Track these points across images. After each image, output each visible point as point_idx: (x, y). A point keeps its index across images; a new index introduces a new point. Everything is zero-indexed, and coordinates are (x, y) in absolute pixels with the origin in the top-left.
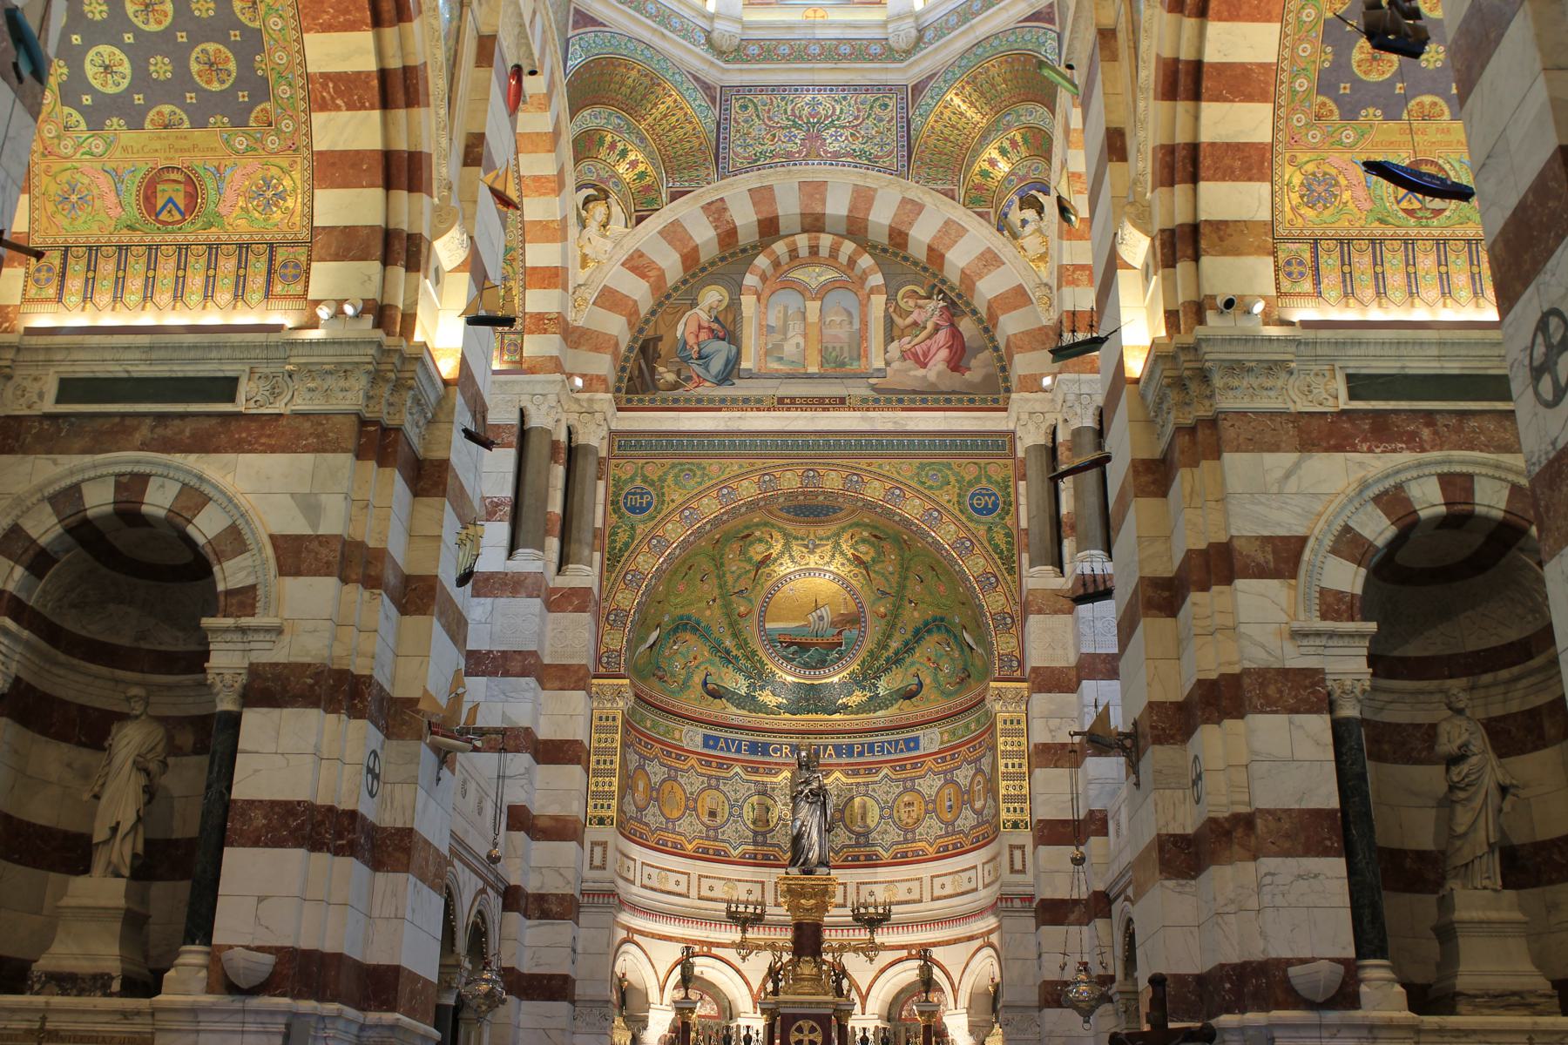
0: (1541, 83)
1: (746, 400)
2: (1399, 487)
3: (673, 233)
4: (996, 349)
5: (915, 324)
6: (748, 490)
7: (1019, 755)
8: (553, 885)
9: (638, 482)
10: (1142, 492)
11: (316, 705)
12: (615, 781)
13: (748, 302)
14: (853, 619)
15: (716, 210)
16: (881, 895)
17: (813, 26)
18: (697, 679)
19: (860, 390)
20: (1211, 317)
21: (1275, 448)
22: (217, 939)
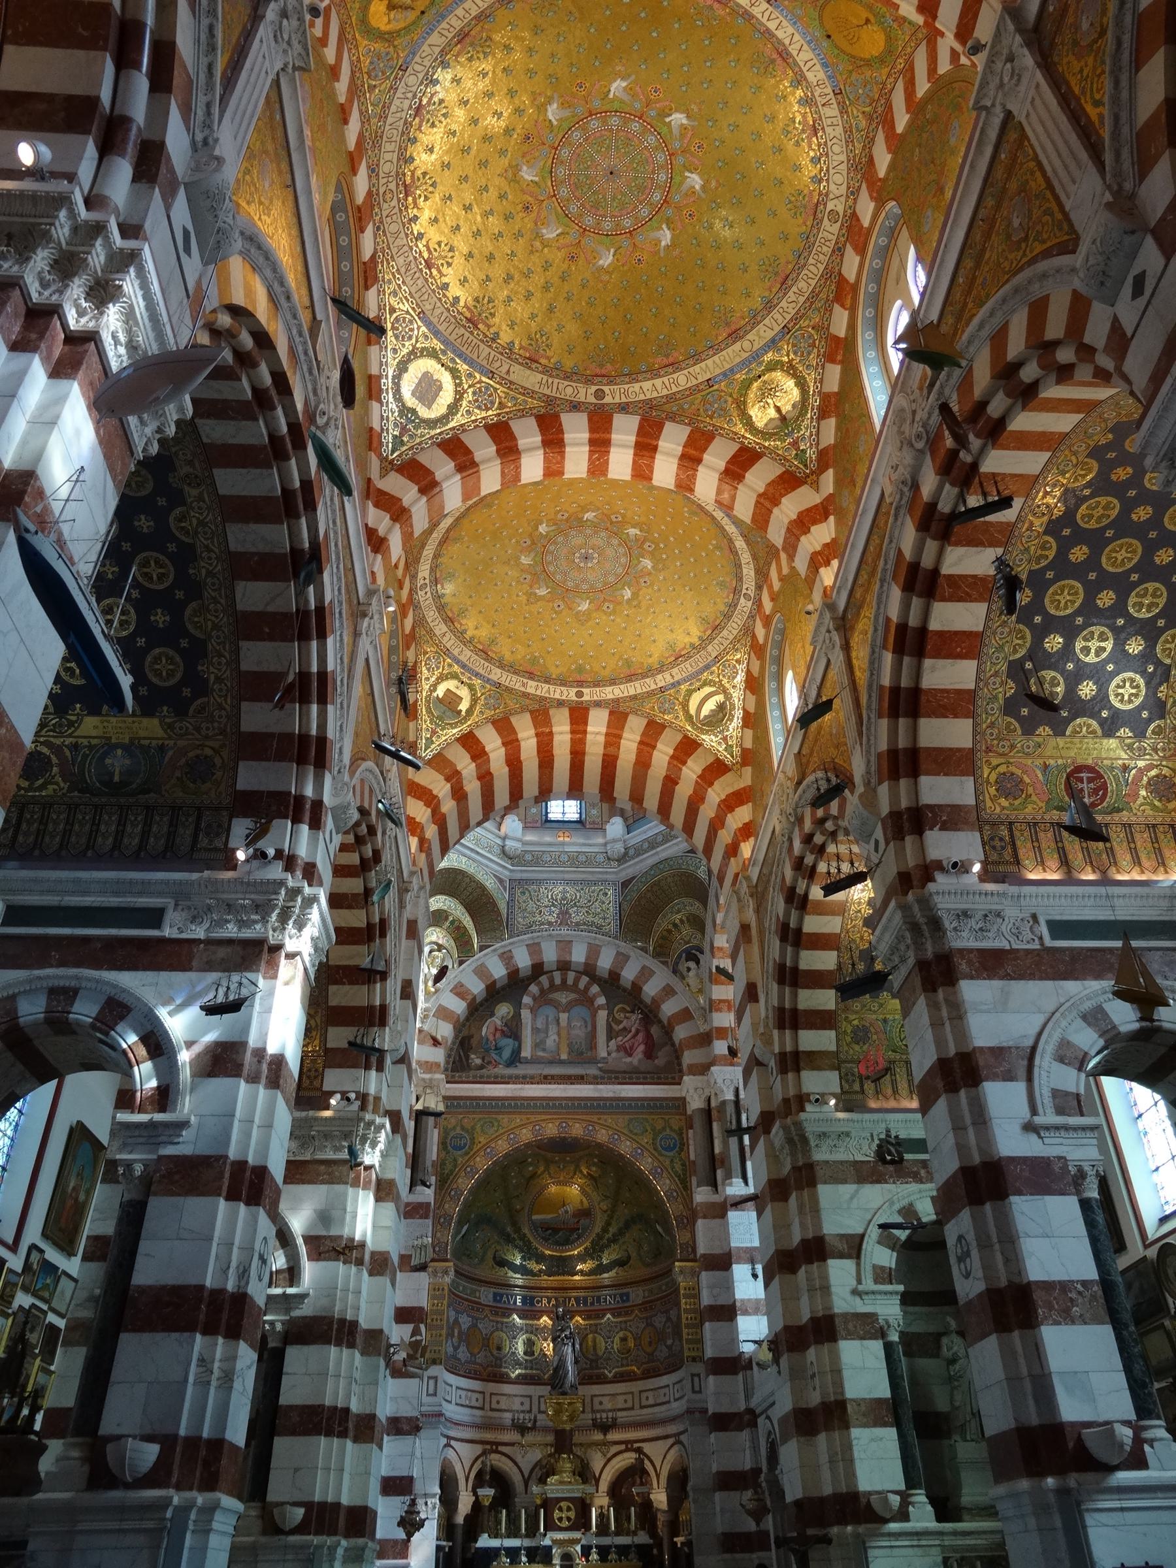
0: (951, 1135)
1: (524, 1077)
2: (911, 1205)
3: (481, 972)
4: (673, 1045)
5: (625, 1029)
6: (526, 1135)
7: (694, 1311)
8: (407, 1411)
9: (458, 1130)
10: (773, 1199)
11: (329, 1342)
12: (444, 1332)
13: (526, 1014)
14: (585, 1213)
15: (507, 957)
16: (608, 1405)
17: (563, 844)
18: (490, 1255)
19: (592, 1071)
20: (809, 1107)
21: (844, 1181)
22: (271, 1497)
